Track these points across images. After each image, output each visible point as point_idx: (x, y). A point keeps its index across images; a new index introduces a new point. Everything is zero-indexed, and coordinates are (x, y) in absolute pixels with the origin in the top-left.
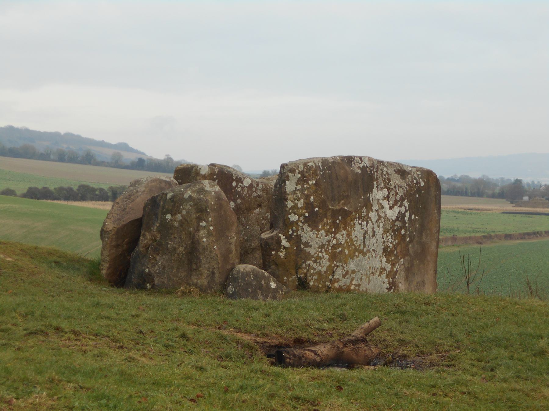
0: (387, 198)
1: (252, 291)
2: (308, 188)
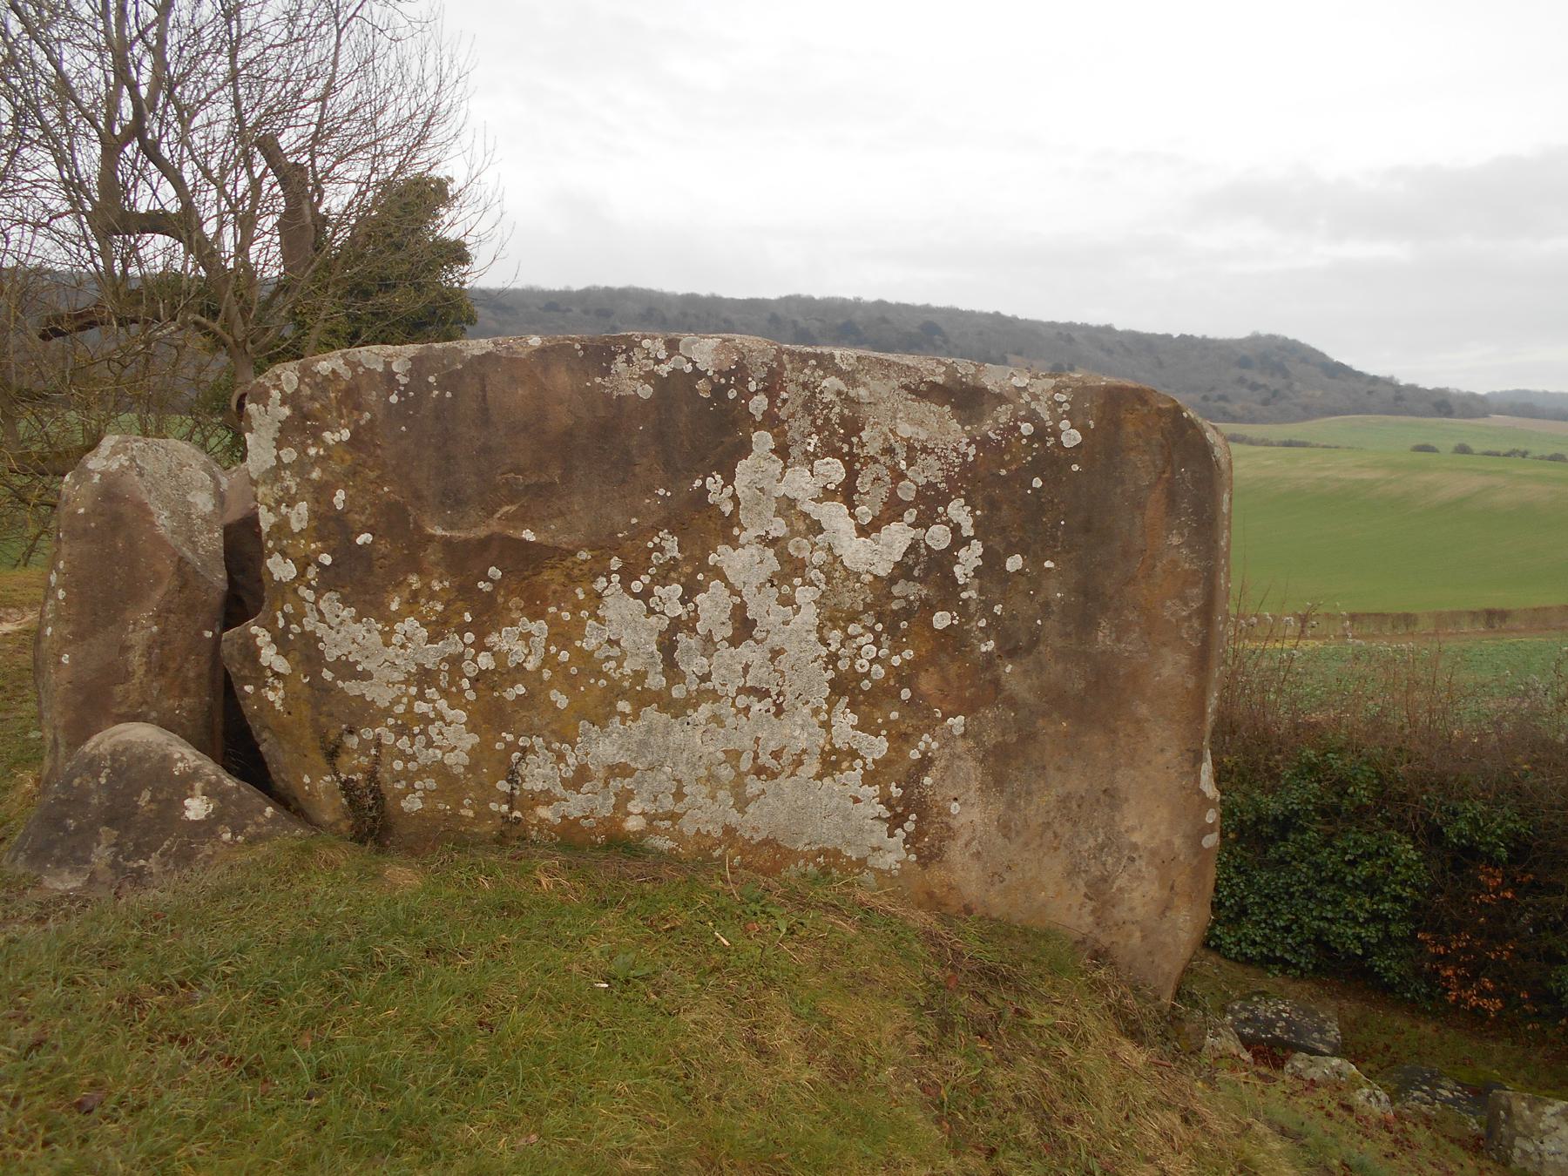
0: (847, 493)
1: (79, 829)
2: (319, 459)
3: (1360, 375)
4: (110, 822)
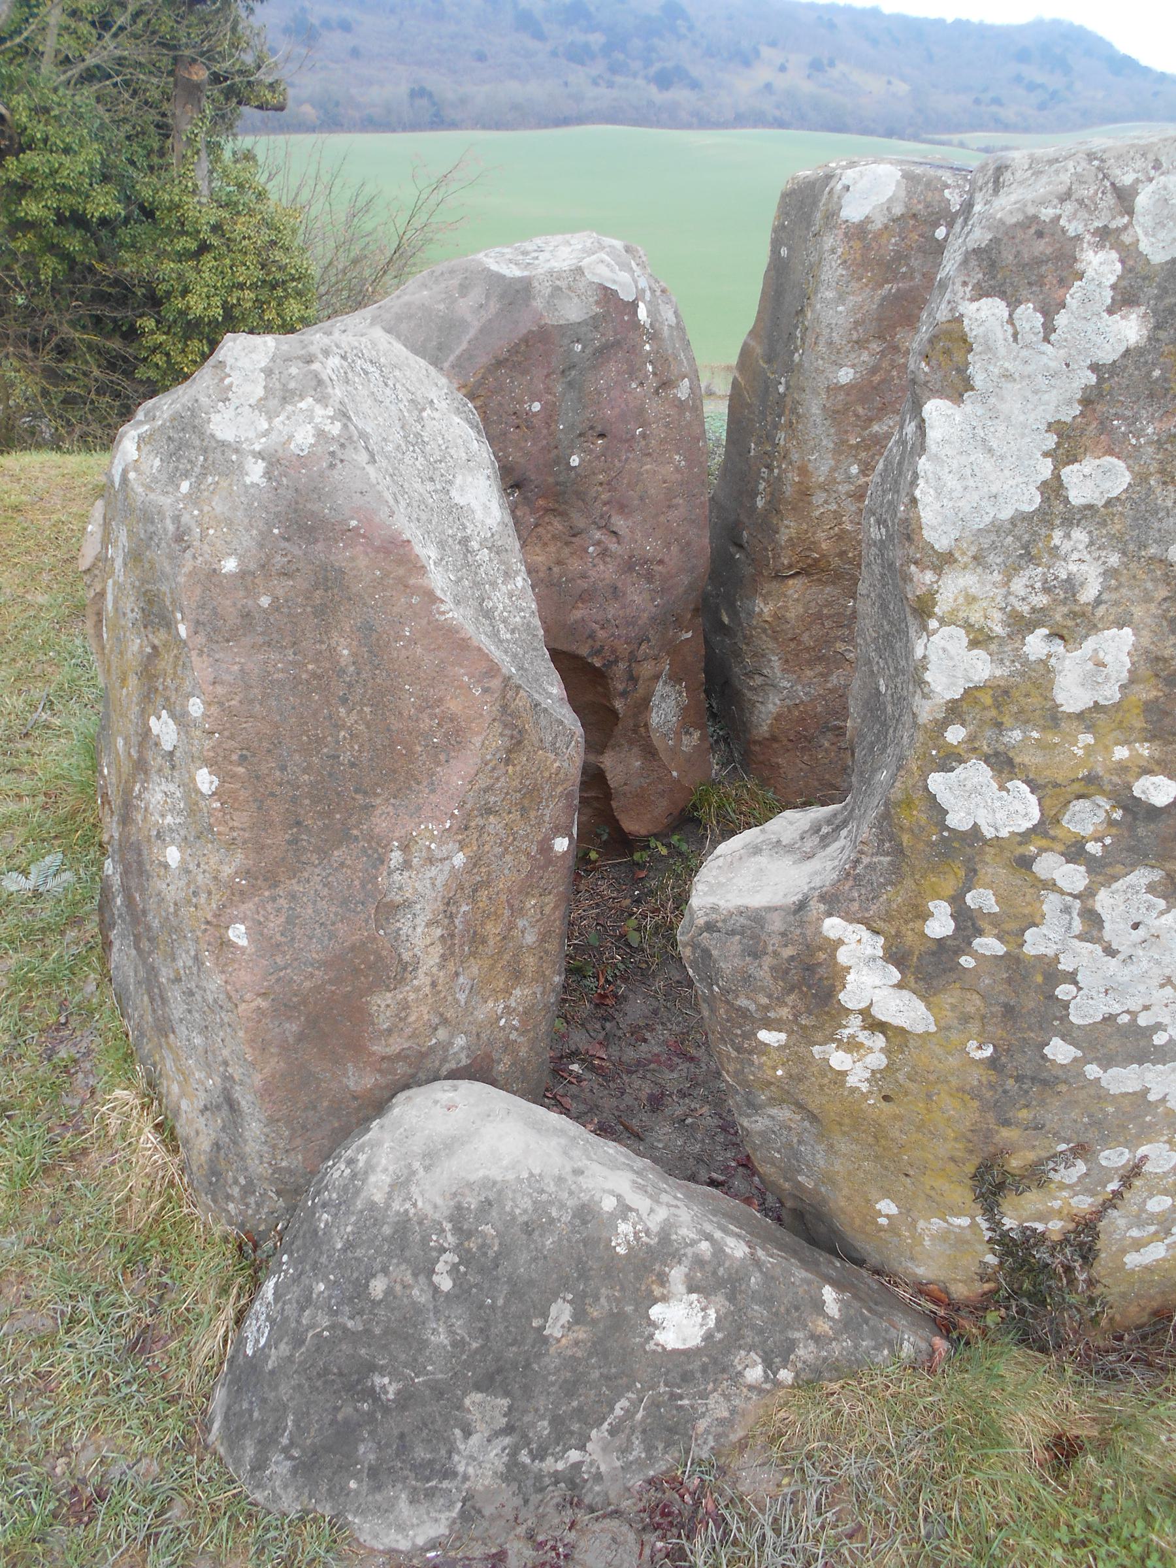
1: (406, 1399)
3: (1147, 71)
4: (489, 1382)
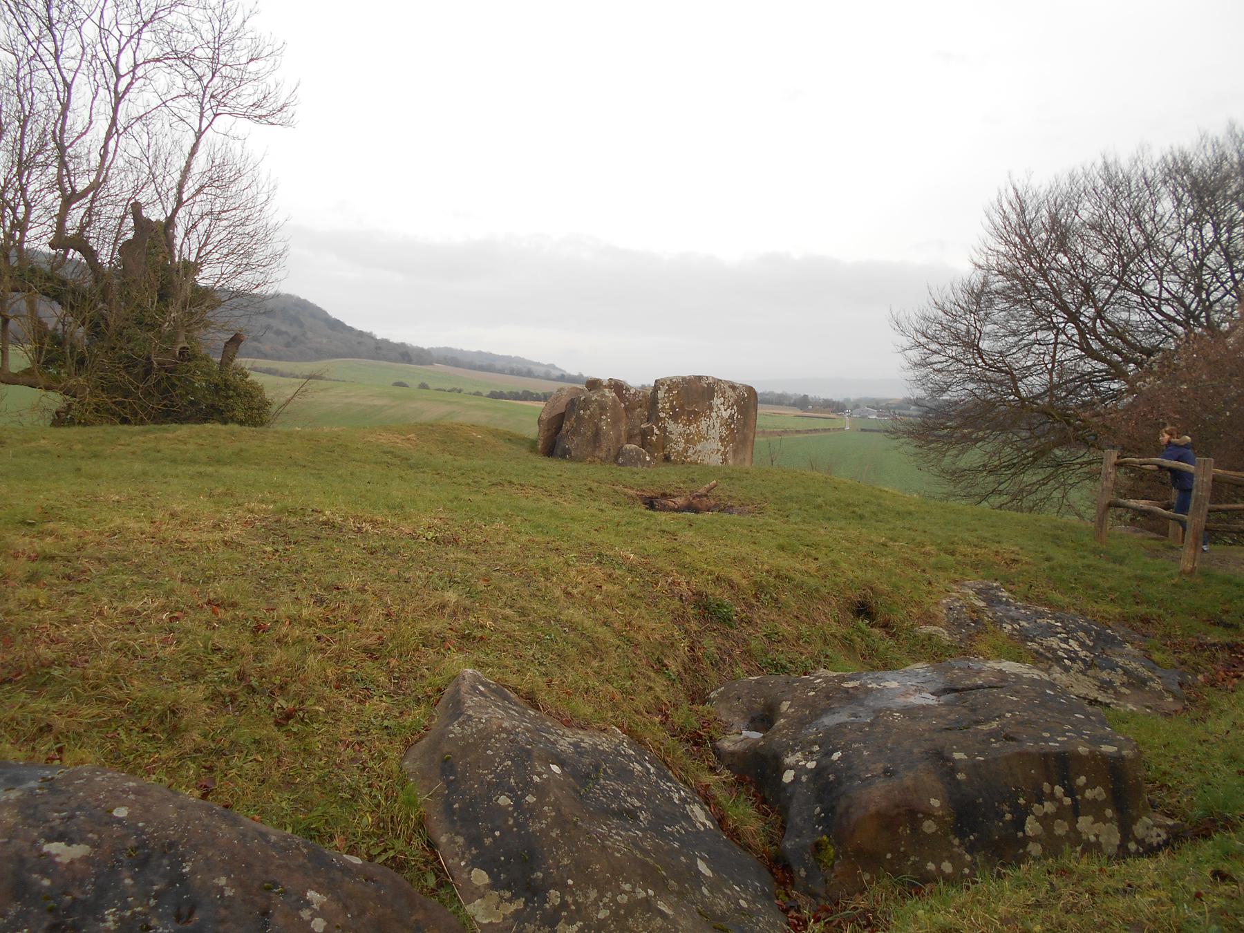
3: (351, 329)
